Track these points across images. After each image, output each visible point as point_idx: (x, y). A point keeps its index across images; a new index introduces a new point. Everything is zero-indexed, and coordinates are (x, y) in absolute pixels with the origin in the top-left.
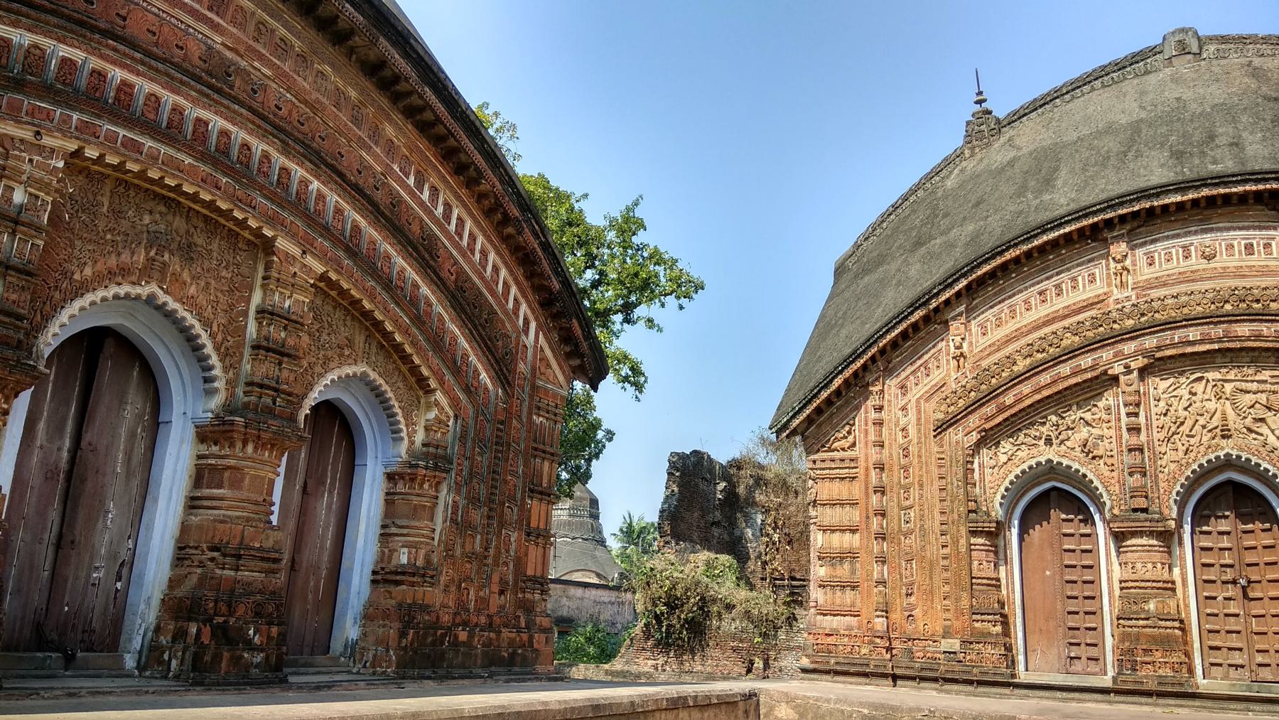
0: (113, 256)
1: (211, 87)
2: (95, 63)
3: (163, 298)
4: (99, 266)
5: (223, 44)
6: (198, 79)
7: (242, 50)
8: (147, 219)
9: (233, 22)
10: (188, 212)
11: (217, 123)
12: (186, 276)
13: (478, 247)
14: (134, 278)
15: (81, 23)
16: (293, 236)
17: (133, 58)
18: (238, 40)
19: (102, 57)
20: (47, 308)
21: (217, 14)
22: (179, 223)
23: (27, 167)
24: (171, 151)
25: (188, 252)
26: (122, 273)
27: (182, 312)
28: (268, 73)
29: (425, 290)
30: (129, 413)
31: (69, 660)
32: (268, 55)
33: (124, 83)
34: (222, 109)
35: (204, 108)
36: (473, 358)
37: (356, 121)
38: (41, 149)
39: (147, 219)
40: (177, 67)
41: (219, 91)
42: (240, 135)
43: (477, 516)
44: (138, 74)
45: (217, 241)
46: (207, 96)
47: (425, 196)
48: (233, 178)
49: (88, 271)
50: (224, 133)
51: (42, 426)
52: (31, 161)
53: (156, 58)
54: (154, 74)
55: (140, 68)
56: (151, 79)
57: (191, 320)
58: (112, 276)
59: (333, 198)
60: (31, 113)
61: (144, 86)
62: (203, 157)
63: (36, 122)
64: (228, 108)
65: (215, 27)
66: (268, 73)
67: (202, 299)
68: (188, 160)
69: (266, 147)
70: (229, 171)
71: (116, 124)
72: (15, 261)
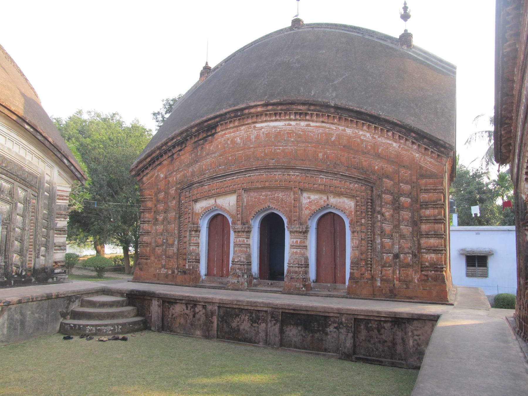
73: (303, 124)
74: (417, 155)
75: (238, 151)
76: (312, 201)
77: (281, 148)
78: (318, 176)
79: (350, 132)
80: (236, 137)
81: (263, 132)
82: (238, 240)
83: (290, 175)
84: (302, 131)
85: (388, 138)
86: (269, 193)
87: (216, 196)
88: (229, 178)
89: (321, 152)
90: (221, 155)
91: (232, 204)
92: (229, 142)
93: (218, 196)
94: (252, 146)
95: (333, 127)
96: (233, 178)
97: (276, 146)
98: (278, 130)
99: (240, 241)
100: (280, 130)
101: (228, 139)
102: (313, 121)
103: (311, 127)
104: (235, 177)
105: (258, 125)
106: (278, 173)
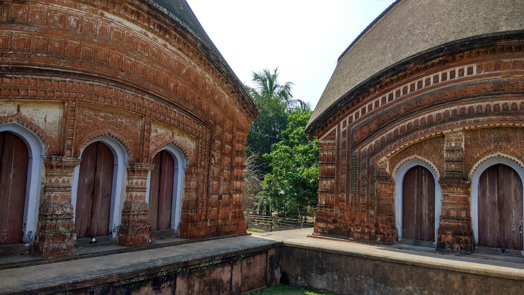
0: (484, 148)
1: (495, 94)
2: (461, 107)
3: (502, 155)
4: (481, 153)
5: (502, 77)
6: (491, 95)
7: (509, 75)
8: (492, 136)
9: (504, 69)
10: (505, 128)
11: (501, 103)
12: (508, 146)
14: (492, 152)
15: (455, 100)
17: (469, 100)
18: (506, 73)
19: (462, 104)
20: (469, 166)
21: (498, 70)
22: (503, 132)
23: (453, 138)
24: (488, 118)
25: (508, 140)
26: (489, 152)
27: (510, 157)
28: (522, 76)
30: (513, 185)
31: (503, 251)
32: (521, 70)
33: (470, 107)
34: (502, 98)
35: (495, 101)
38: (455, 132)
39: (492, 136)
40: (484, 95)
41: (499, 94)
42: (510, 102)
44: (473, 103)
45: (518, 133)
46: (495, 97)
48: (511, 116)
49: (478, 155)
50: (506, 104)
51: (488, 192)
52: (453, 136)
53: (477, 96)
54: (477, 101)
55: (473, 101)
56: (477, 102)
57: (513, 158)
58: (485, 154)
60: (449, 126)
61: (475, 105)
62: (498, 115)
63: (450, 127)
64: (503, 97)
66: (522, 76)
67: (516, 152)
68: (494, 117)
69: (521, 101)
70: (509, 114)
71: (470, 118)
72: (456, 159)
73: (161, 41)
74: (238, 110)
75: (74, 39)
76: (158, 135)
77: (133, 59)
78: (172, 108)
79: (199, 70)
80: (70, 15)
81: (112, 28)
82: (60, 180)
83: (143, 99)
84: (157, 49)
85: (224, 89)
86: (110, 115)
87: (21, 102)
88: (58, 79)
89: (173, 82)
90: (41, 34)
91: (52, 122)
92: (56, 18)
93: (26, 102)
94: (96, 41)
95: (187, 59)
96: (64, 79)
97: (127, 54)
98: (131, 34)
99: (64, 181)
100: (132, 36)
101: (56, 12)
102: (170, 44)
103: (167, 48)
104: (68, 79)
105: (107, 14)
106: (131, 92)
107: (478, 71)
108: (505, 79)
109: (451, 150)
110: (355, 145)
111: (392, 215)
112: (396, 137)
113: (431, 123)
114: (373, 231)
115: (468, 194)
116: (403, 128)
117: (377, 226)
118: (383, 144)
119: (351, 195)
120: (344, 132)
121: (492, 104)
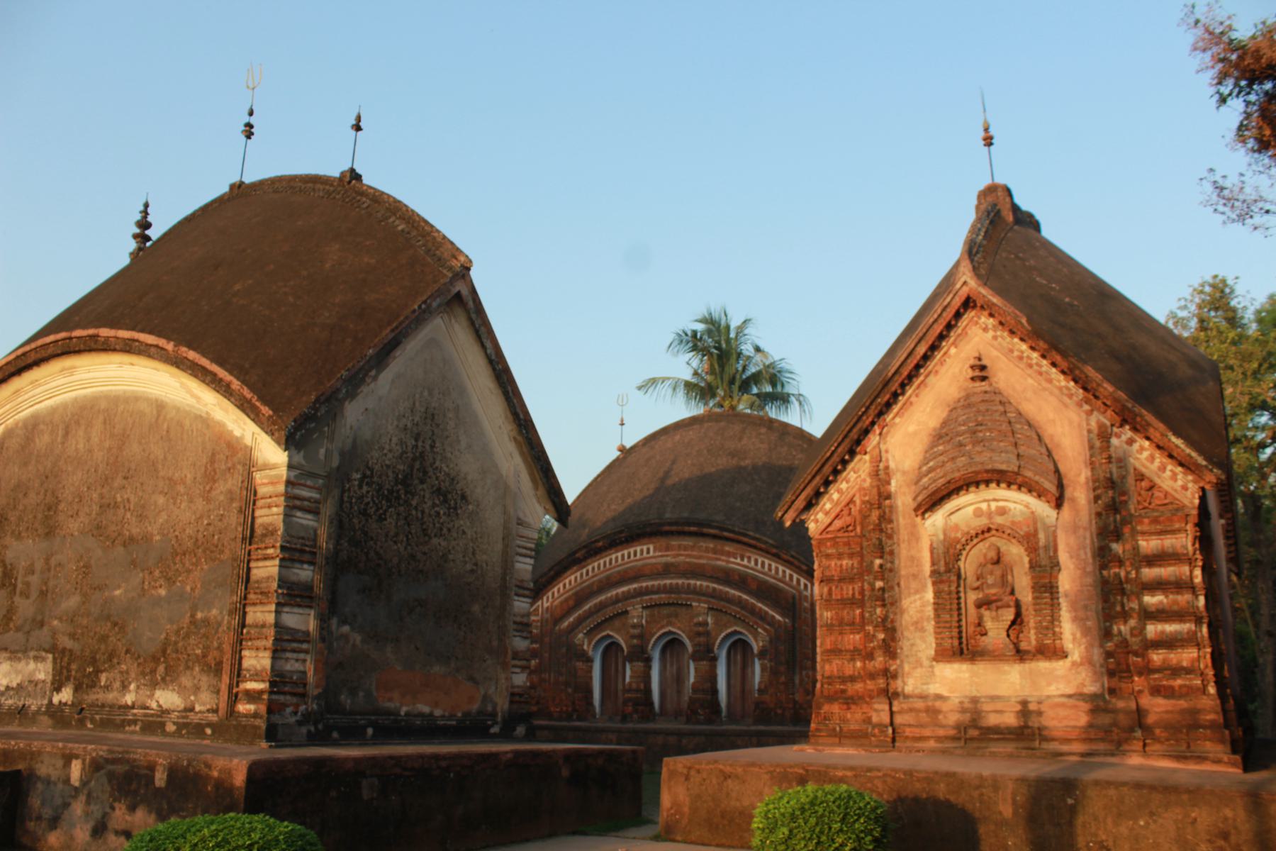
11: (668, 582)
13: (773, 567)
16: (694, 601)
25: (676, 616)
26: (662, 627)
29: (745, 597)
36: (771, 612)
37: (715, 553)
42: (674, 581)
43: (782, 669)
47: (745, 562)
59: (705, 584)
65: (667, 556)
70: (675, 593)
107: (654, 551)
108: (673, 560)
109: (634, 626)
110: (558, 620)
111: (589, 691)
112: (590, 614)
113: (617, 600)
114: (570, 709)
115: (650, 668)
116: (595, 605)
117: (573, 703)
118: (580, 621)
119: (552, 675)
120: (547, 608)
121: (662, 582)
